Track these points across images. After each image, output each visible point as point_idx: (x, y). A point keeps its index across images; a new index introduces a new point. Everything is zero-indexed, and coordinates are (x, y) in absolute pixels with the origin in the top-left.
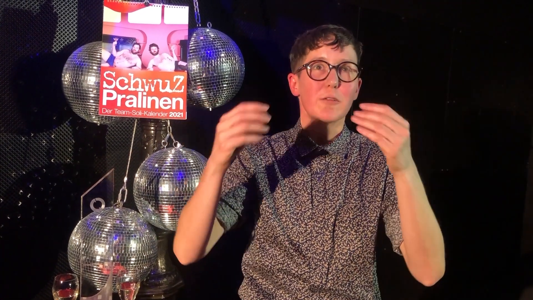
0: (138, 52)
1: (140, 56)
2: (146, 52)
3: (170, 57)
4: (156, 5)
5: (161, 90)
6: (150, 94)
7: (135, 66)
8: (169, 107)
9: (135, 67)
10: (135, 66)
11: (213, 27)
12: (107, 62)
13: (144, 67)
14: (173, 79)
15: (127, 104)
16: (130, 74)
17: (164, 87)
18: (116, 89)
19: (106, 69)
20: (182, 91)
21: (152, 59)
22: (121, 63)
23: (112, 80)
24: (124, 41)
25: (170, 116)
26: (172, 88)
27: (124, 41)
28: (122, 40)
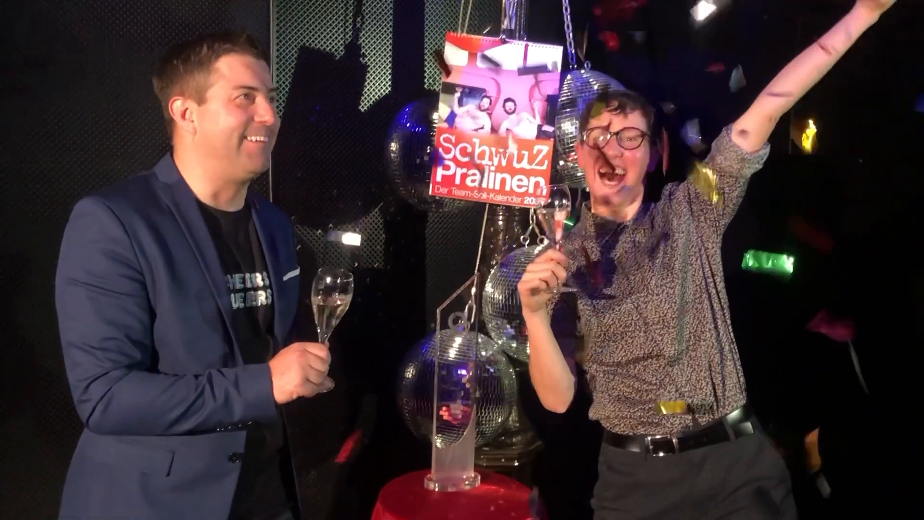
0: (488, 109)
1: (490, 115)
2: (499, 110)
3: (531, 119)
4: (517, 42)
5: (515, 165)
6: (499, 169)
7: (482, 128)
8: (523, 190)
9: (481, 131)
10: (482, 128)
11: (592, 69)
12: (446, 121)
13: (494, 130)
14: (533, 149)
15: (468, 181)
16: (475, 140)
17: (519, 161)
18: (455, 159)
19: (442, 131)
20: (544, 167)
21: (507, 118)
22: (465, 123)
23: (451, 146)
24: (471, 92)
25: (525, 202)
26: (530, 162)
27: (471, 92)
28: (467, 90)
